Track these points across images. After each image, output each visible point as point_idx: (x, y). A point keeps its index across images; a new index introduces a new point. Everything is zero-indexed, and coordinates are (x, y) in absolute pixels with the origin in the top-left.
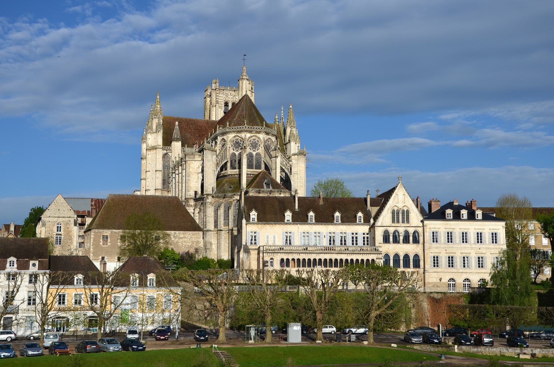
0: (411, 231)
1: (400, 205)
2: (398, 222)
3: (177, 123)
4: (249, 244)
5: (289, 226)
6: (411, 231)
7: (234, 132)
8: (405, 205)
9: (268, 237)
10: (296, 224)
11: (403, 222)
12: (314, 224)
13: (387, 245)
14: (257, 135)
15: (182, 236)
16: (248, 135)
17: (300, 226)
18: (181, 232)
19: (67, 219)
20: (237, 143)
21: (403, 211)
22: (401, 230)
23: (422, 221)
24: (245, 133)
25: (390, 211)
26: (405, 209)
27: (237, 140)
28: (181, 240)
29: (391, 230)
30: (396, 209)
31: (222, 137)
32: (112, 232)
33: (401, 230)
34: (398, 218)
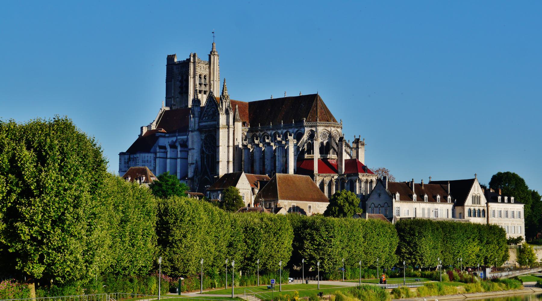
0: (481, 209)
1: (476, 193)
2: (475, 204)
3: (237, 106)
4: (396, 216)
5: (415, 203)
6: (481, 209)
7: (323, 126)
8: (478, 192)
9: (405, 211)
10: (420, 203)
11: (477, 204)
12: (428, 203)
13: (470, 218)
14: (337, 129)
15: (321, 206)
16: (333, 129)
17: (421, 203)
18: (321, 203)
19: (247, 191)
20: (324, 134)
21: (478, 196)
22: (477, 208)
23: (487, 203)
24: (331, 127)
25: (471, 196)
26: (478, 195)
27: (324, 132)
28: (321, 209)
29: (472, 208)
30: (474, 195)
31: (310, 129)
32: (288, 202)
33: (477, 208)
34: (475, 202)
